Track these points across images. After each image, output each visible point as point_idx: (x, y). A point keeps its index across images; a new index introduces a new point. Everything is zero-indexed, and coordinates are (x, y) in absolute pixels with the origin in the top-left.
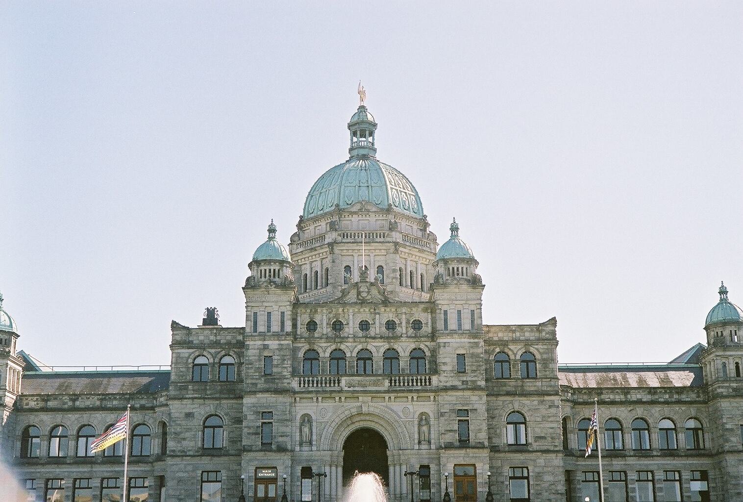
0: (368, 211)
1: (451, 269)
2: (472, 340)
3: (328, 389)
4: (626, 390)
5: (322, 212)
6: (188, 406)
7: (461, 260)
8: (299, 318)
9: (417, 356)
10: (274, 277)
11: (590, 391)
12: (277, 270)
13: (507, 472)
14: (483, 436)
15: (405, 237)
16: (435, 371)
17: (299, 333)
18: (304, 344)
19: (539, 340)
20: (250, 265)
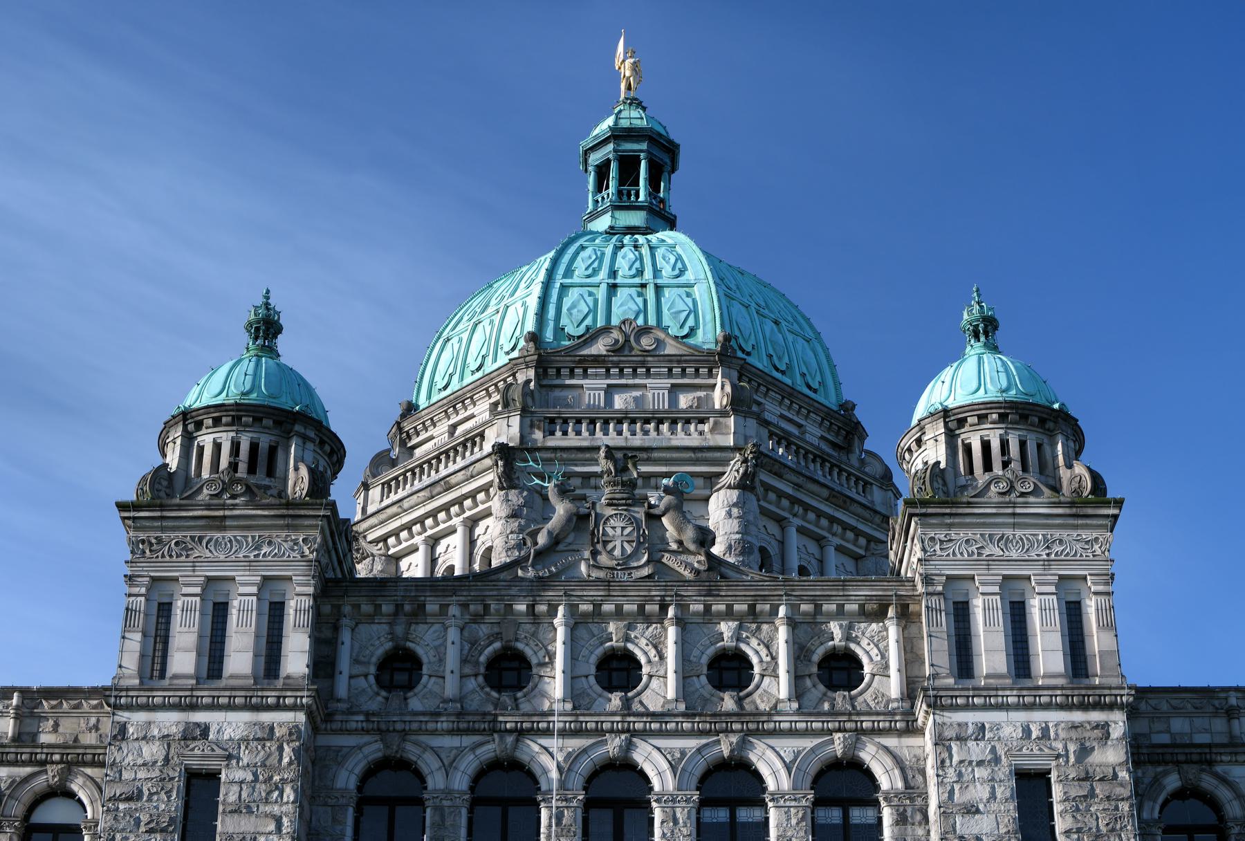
2: (1077, 716)
5: (479, 375)
8: (346, 636)
10: (252, 469)
17: (342, 690)
18: (367, 738)
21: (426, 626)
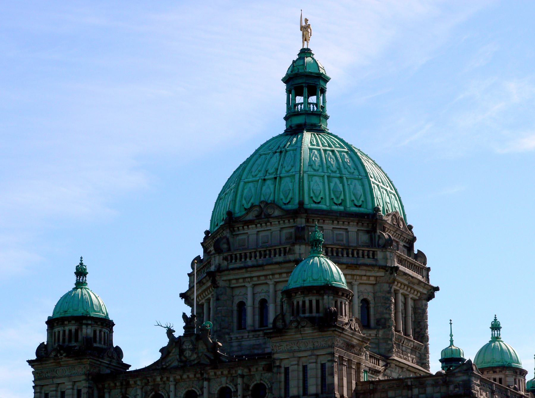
0: (269, 216)
1: (295, 303)
7: (307, 290)
12: (73, 331)
21: (132, 389)
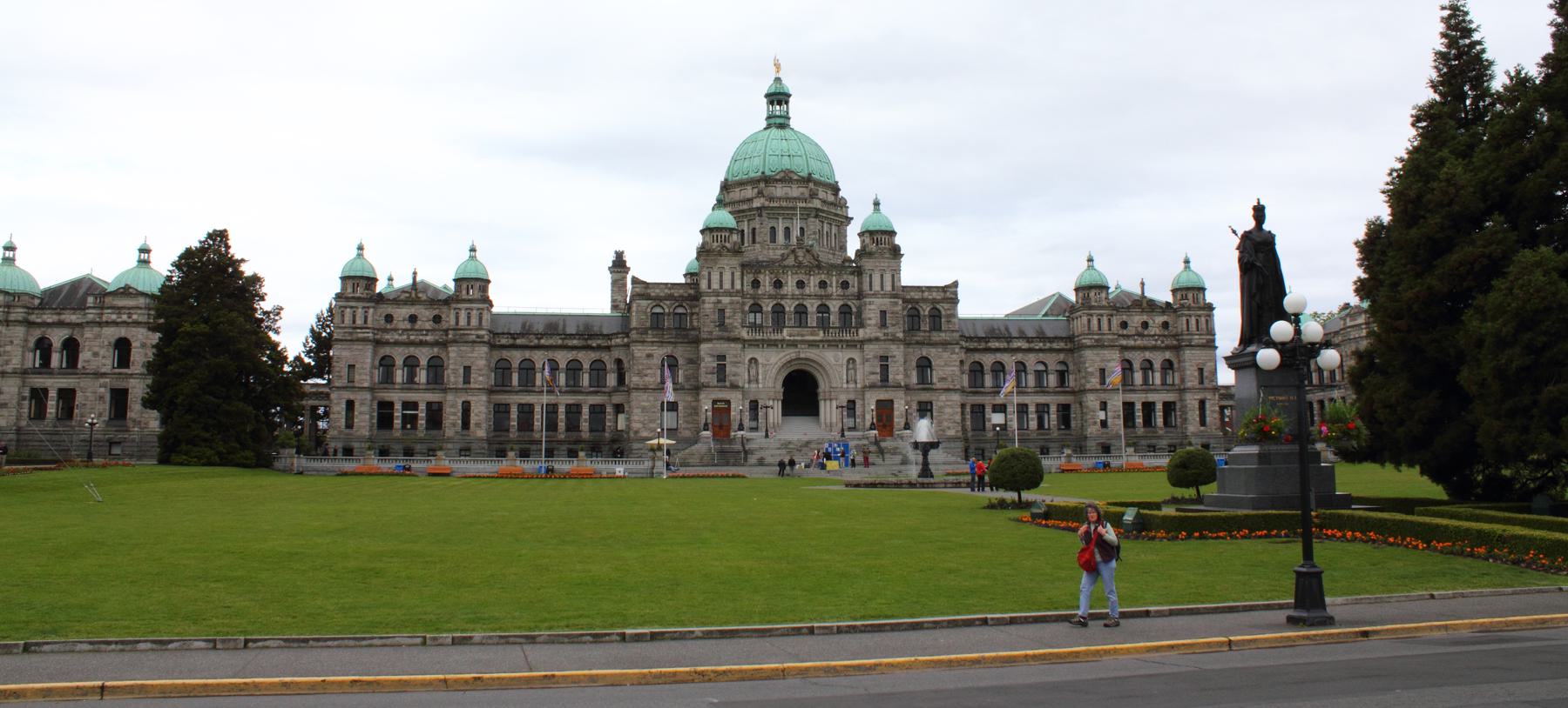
3: (773, 337)
4: (1009, 339)
6: (649, 349)
9: (845, 311)
11: (980, 339)
13: (915, 406)
14: (900, 377)
15: (824, 202)
16: (861, 325)
19: (945, 300)
20: (702, 232)
